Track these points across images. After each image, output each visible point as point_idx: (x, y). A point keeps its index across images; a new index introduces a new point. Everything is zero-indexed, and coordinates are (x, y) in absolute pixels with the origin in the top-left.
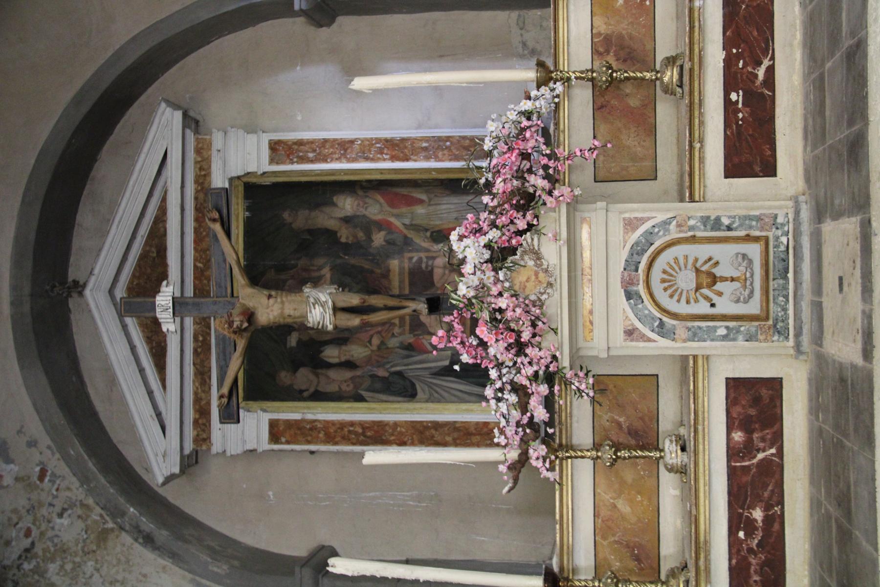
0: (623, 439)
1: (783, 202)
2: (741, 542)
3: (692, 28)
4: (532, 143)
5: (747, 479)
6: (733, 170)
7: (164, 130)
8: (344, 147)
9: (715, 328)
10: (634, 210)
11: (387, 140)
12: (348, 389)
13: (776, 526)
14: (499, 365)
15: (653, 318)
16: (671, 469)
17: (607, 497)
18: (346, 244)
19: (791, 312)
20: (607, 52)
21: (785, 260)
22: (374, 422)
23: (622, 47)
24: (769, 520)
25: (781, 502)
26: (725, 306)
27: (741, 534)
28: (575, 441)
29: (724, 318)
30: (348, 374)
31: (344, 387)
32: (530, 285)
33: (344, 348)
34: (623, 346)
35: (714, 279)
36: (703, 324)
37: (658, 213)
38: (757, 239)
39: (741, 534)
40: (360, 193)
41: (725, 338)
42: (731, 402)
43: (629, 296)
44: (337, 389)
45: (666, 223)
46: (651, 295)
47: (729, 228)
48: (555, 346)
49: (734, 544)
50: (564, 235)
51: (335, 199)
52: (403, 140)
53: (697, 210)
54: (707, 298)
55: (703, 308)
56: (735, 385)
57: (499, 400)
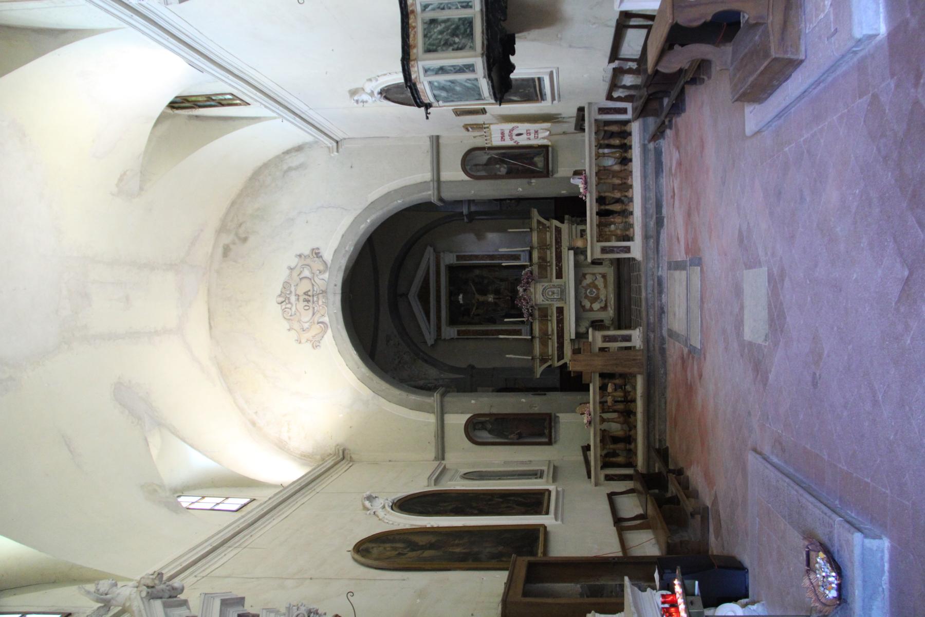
6: (557, 278)
7: (429, 253)
8: (477, 257)
37: (546, 284)
56: (557, 308)
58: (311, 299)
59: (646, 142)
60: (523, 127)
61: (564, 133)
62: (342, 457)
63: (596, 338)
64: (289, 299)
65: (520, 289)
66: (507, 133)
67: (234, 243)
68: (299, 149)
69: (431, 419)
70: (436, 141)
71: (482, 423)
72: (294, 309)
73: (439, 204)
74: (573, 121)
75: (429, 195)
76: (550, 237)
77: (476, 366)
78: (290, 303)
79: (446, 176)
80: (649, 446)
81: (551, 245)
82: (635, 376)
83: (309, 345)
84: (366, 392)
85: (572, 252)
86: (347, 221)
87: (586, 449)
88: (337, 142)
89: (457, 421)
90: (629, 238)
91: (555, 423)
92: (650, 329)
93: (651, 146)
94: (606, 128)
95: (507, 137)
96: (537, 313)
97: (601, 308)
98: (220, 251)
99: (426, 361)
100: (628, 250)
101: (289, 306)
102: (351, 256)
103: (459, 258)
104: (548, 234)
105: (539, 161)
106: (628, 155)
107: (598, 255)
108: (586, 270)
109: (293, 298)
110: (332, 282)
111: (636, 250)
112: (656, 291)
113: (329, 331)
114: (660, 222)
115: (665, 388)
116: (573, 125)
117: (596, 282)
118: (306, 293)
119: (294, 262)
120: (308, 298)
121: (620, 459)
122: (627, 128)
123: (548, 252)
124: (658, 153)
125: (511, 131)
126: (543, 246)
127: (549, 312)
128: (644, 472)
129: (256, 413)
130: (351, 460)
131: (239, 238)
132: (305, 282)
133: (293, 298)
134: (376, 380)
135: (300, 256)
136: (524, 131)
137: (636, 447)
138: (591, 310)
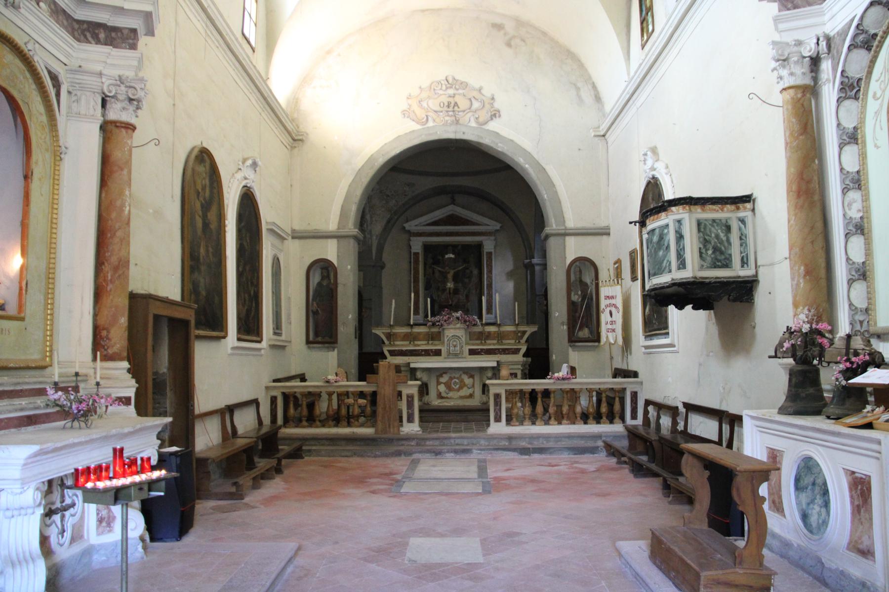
7: (495, 226)
8: (490, 271)
37: (463, 339)
56: (440, 350)
58: (451, 109)
59: (604, 438)
60: (618, 317)
61: (612, 358)
62: (295, 139)
63: (411, 388)
64: (451, 87)
65: (459, 314)
66: (612, 301)
67: (505, 34)
68: (598, 98)
69: (332, 226)
70: (604, 232)
71: (328, 277)
72: (441, 92)
73: (543, 235)
74: (625, 367)
75: (552, 226)
76: (509, 344)
77: (385, 273)
78: (447, 88)
79: (570, 241)
80: (305, 439)
81: (502, 344)
82: (373, 426)
83: (405, 107)
84: (359, 162)
85: (495, 364)
86: (527, 144)
87: (303, 378)
88: (604, 136)
89: (330, 251)
90: (509, 420)
91: (328, 348)
92: (420, 441)
93: (600, 443)
94: (617, 399)
95: (608, 302)
96: (435, 330)
98: (498, 21)
99: (389, 222)
100: (498, 419)
101: (444, 87)
102: (492, 148)
103: (490, 254)
104: (512, 341)
105: (585, 333)
106: (591, 420)
107: (493, 391)
108: (477, 378)
109: (451, 92)
110: (468, 130)
111: (498, 428)
112: (457, 447)
113: (418, 127)
114: (524, 451)
115: (362, 456)
116: (619, 366)
117: (465, 388)
118: (456, 104)
119: (487, 92)
120: (452, 107)
121: (292, 411)
122: (617, 420)
123: (495, 342)
124: (593, 450)
125: (615, 306)
126: (500, 337)
127: (437, 342)
128: (279, 435)
129: (339, 55)
130: (293, 148)
131: (511, 39)
132: (468, 103)
133: (451, 92)
134: (370, 173)
135: (493, 99)
136: (614, 318)
137: (304, 427)
138: (439, 383)
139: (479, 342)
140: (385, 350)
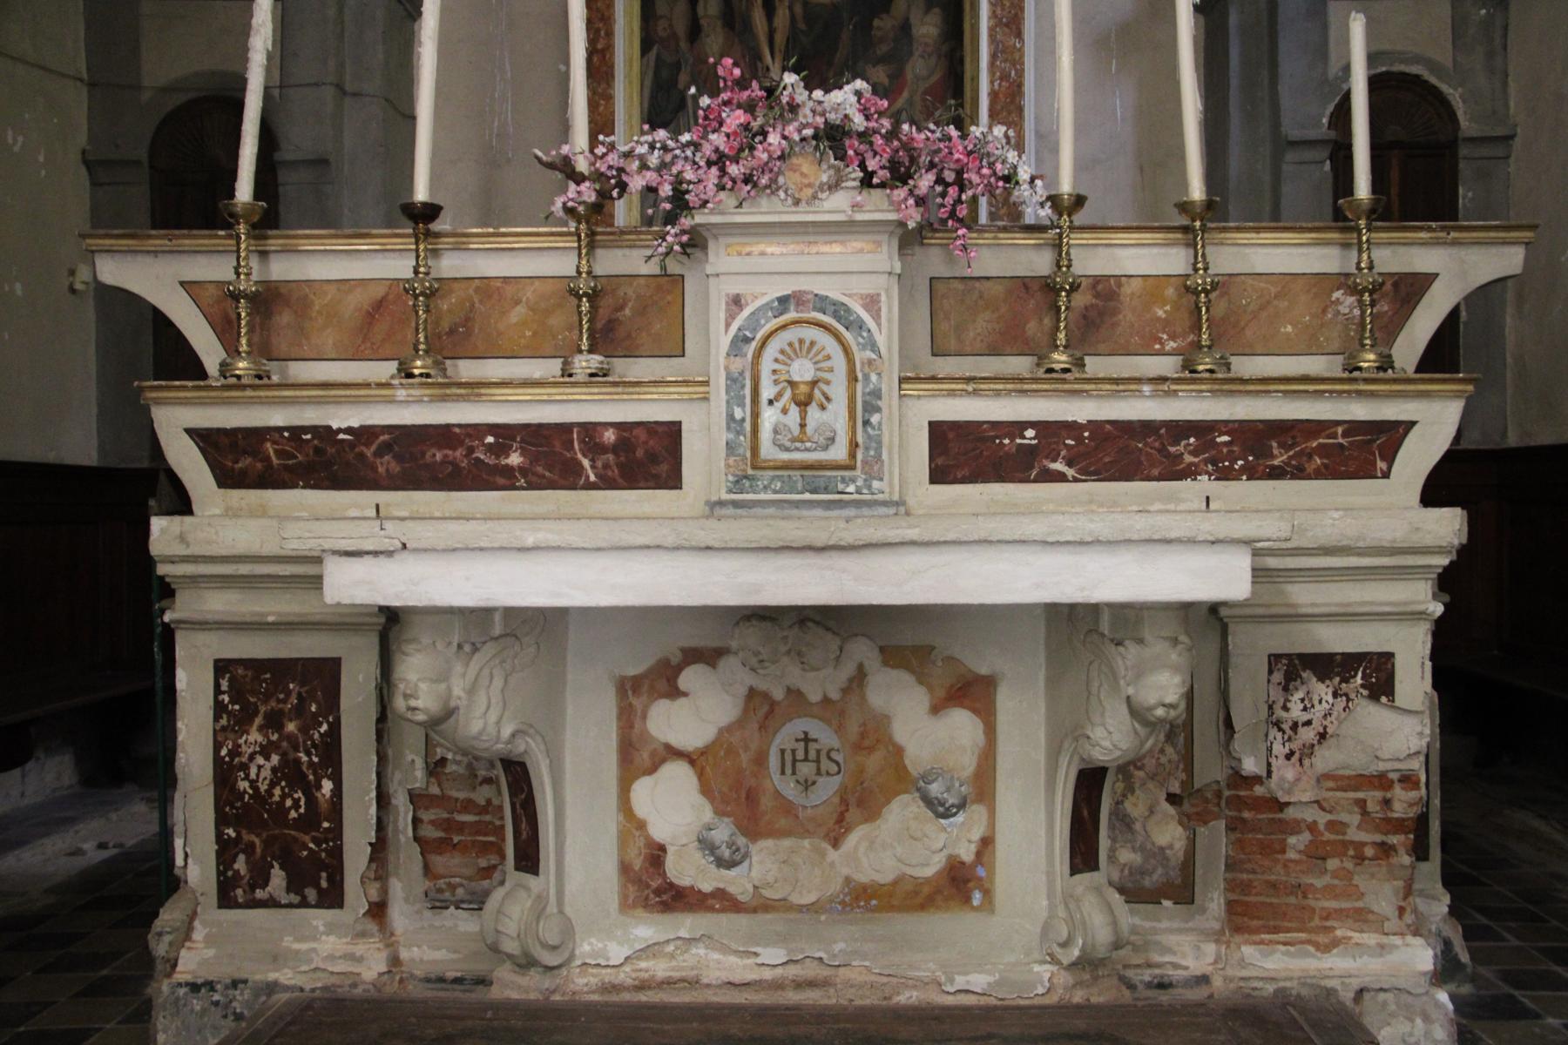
0: (604, 313)
1: (897, 488)
2: (482, 439)
3: (1116, 381)
4: (975, 179)
5: (558, 447)
6: (939, 431)
9: (742, 405)
10: (890, 306)
11: (1020, 85)
12: (660, 29)
13: (501, 481)
14: (696, 146)
15: (755, 330)
16: (565, 363)
17: (529, 294)
18: (870, 26)
19: (762, 496)
20: (1097, 295)
21: (826, 490)
22: (612, 67)
23: (1101, 314)
24: (509, 471)
25: (531, 486)
26: (769, 417)
27: (490, 439)
28: (599, 252)
29: (756, 415)
30: (681, 27)
31: (662, 24)
32: (796, 177)
33: (719, 23)
34: (720, 291)
35: (803, 404)
36: (747, 391)
37: (885, 335)
38: (853, 455)
39: (490, 439)
40: (945, 48)
41: (731, 417)
42: (651, 428)
43: (784, 300)
44: (659, 12)
45: (873, 346)
46: (784, 327)
47: (866, 423)
48: (719, 210)
49: (478, 430)
50: (859, 217)
51: (937, 10)
52: (1020, 110)
53: (889, 386)
54: (779, 395)
55: (767, 392)
56: (672, 431)
57: (652, 147)
76: (1282, 384)
85: (1224, 578)
97: (657, 855)
108: (1022, 712)
117: (902, 811)
123: (1166, 365)
126: (1207, 324)
138: (637, 757)
139: (1020, 364)
140: (176, 422)
